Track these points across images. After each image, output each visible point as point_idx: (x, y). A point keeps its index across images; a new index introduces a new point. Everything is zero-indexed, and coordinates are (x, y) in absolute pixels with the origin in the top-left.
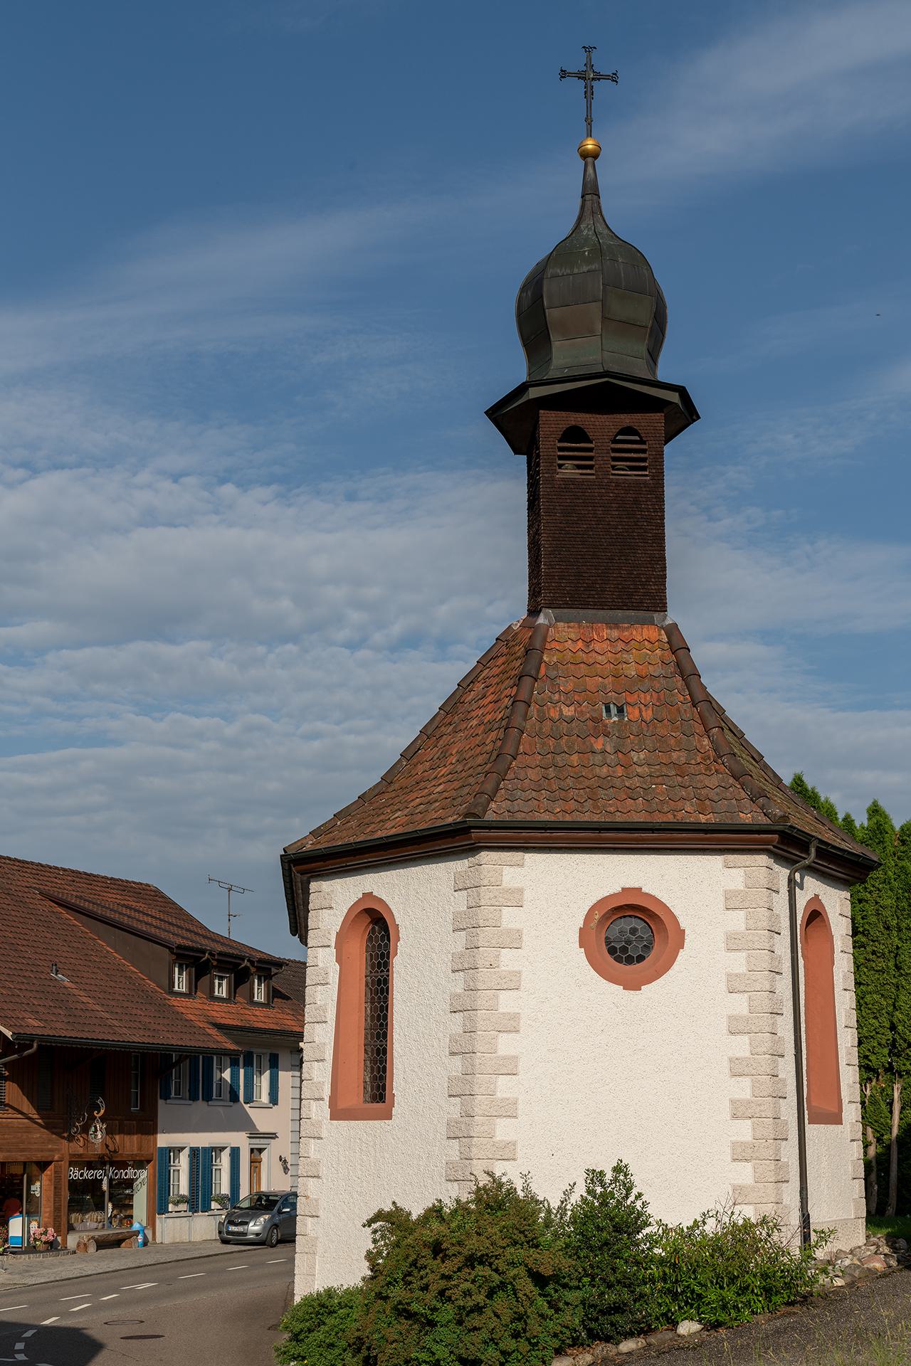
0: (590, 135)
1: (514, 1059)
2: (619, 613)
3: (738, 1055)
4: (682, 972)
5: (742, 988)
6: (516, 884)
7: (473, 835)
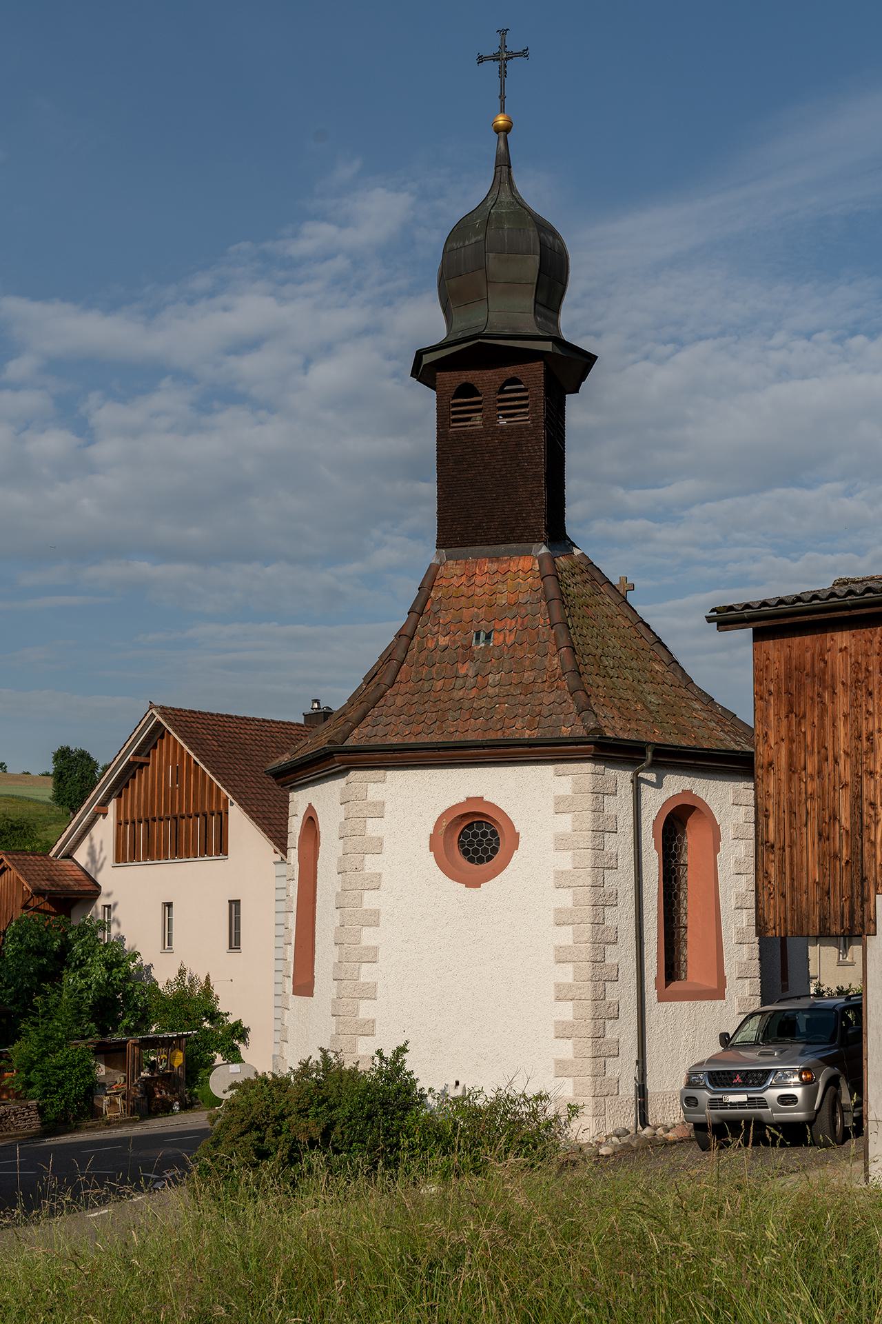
0: (502, 111)
1: (375, 949)
2: (503, 547)
3: (562, 944)
4: (515, 870)
5: (568, 883)
6: (378, 798)
7: (336, 758)
